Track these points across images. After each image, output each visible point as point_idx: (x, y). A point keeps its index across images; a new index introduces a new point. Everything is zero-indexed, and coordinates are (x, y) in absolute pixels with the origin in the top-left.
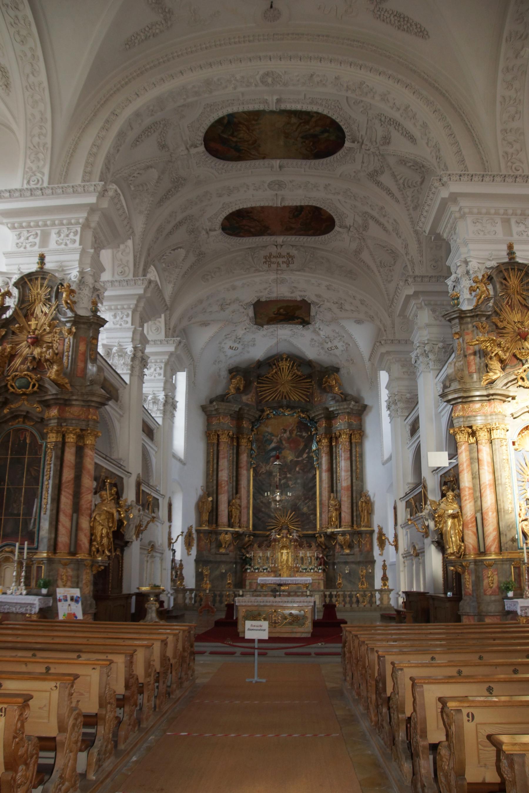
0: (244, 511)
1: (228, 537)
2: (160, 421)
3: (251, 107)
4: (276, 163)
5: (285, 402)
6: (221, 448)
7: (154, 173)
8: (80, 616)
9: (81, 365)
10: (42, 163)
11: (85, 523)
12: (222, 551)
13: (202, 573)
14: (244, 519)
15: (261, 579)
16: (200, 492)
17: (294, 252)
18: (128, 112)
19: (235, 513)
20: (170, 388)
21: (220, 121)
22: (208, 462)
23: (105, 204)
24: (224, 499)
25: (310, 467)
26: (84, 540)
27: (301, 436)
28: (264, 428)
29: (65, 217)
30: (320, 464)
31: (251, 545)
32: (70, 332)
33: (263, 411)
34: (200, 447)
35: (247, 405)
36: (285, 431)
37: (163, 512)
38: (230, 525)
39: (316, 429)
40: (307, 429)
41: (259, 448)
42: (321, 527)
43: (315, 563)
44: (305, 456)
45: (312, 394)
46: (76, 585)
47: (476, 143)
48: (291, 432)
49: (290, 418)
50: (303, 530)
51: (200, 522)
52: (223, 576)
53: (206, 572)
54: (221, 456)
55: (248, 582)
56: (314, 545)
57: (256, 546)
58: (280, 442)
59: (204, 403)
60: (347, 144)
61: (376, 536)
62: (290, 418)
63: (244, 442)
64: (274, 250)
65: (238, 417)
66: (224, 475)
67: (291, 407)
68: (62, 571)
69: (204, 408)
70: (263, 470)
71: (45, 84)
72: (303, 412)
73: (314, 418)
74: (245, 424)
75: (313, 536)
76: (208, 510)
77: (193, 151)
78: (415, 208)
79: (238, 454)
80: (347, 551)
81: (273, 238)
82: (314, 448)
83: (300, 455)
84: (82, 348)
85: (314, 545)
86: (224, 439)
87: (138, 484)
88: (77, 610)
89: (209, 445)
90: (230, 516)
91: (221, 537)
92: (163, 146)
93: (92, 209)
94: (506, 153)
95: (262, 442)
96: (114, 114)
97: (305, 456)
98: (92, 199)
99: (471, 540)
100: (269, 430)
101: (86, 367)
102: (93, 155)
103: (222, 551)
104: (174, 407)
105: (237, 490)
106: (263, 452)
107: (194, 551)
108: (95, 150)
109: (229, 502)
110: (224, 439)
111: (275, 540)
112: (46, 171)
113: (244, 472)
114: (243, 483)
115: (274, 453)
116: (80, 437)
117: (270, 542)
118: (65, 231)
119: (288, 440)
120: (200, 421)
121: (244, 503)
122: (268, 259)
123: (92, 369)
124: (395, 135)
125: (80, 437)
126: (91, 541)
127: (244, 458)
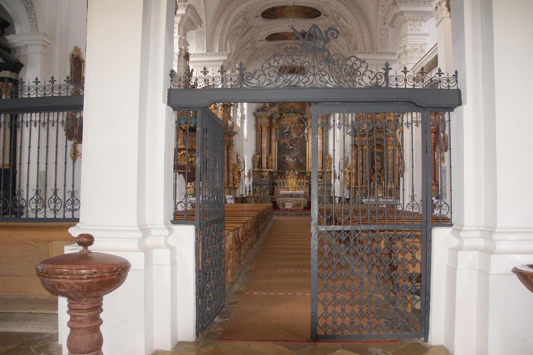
0: (274, 161)
1: (266, 174)
2: (239, 126)
3: (282, 5)
4: (292, 20)
5: (292, 110)
6: (263, 132)
7: (241, 29)
8: (233, 203)
9: (226, 121)
10: (203, 39)
11: (231, 175)
12: (264, 179)
13: (255, 189)
14: (274, 165)
15: (282, 192)
16: (254, 153)
17: (298, 46)
18: (234, 15)
19: (270, 163)
20: (242, 109)
21: (269, 9)
22: (257, 139)
23: (230, 60)
24: (264, 156)
25: (303, 142)
26: (231, 180)
27: (300, 126)
28: (282, 122)
29: (214, 63)
30: (308, 140)
31: (277, 177)
32: (221, 110)
33: (282, 114)
34: (253, 132)
35: (275, 112)
36: (292, 124)
37: (242, 164)
38: (268, 168)
39: (307, 123)
40: (303, 123)
41: (280, 132)
42: (308, 169)
43: (305, 184)
44: (302, 136)
45: (305, 106)
46: (230, 194)
47: (370, 32)
48: (295, 125)
49: (295, 118)
50: (300, 170)
51: (254, 167)
52: (264, 191)
53: (257, 189)
54: (263, 136)
55: (275, 193)
56: (305, 177)
57: (279, 177)
58: (290, 129)
59: (254, 112)
60: (322, 16)
61: (333, 173)
62: (295, 118)
63: (273, 130)
64: (289, 46)
65: (271, 118)
66: (265, 145)
67: (295, 112)
68: (226, 190)
69: (254, 114)
70: (282, 142)
71: (203, 8)
72: (301, 115)
73: (305, 118)
74: (274, 121)
75: (305, 173)
76: (258, 162)
77: (257, 19)
78: (350, 43)
79: (270, 135)
80: (320, 180)
81: (289, 41)
82: (306, 132)
83: (299, 135)
84: (226, 115)
85: (305, 177)
86: (264, 129)
87: (237, 156)
88: (232, 202)
89: (257, 131)
90: (267, 164)
91: (263, 174)
92: (244, 19)
93: (225, 61)
94: (380, 39)
95: (281, 129)
96: (228, 16)
97: (302, 136)
98: (225, 58)
99: (353, 181)
100: (285, 123)
101: (228, 122)
102: (222, 35)
103: (264, 179)
104: (245, 119)
105: (270, 151)
106: (282, 134)
107: (252, 180)
108: (222, 32)
109: (267, 158)
110: (264, 129)
111: (288, 175)
112: (205, 42)
113: (273, 144)
114: (273, 148)
115: (287, 134)
116: (228, 147)
117: (285, 176)
118: (214, 68)
119: (294, 128)
120: (253, 119)
121: (274, 157)
122: (286, 49)
123: (230, 123)
124: (341, 18)
125: (228, 147)
126: (233, 181)
127: (273, 137)
